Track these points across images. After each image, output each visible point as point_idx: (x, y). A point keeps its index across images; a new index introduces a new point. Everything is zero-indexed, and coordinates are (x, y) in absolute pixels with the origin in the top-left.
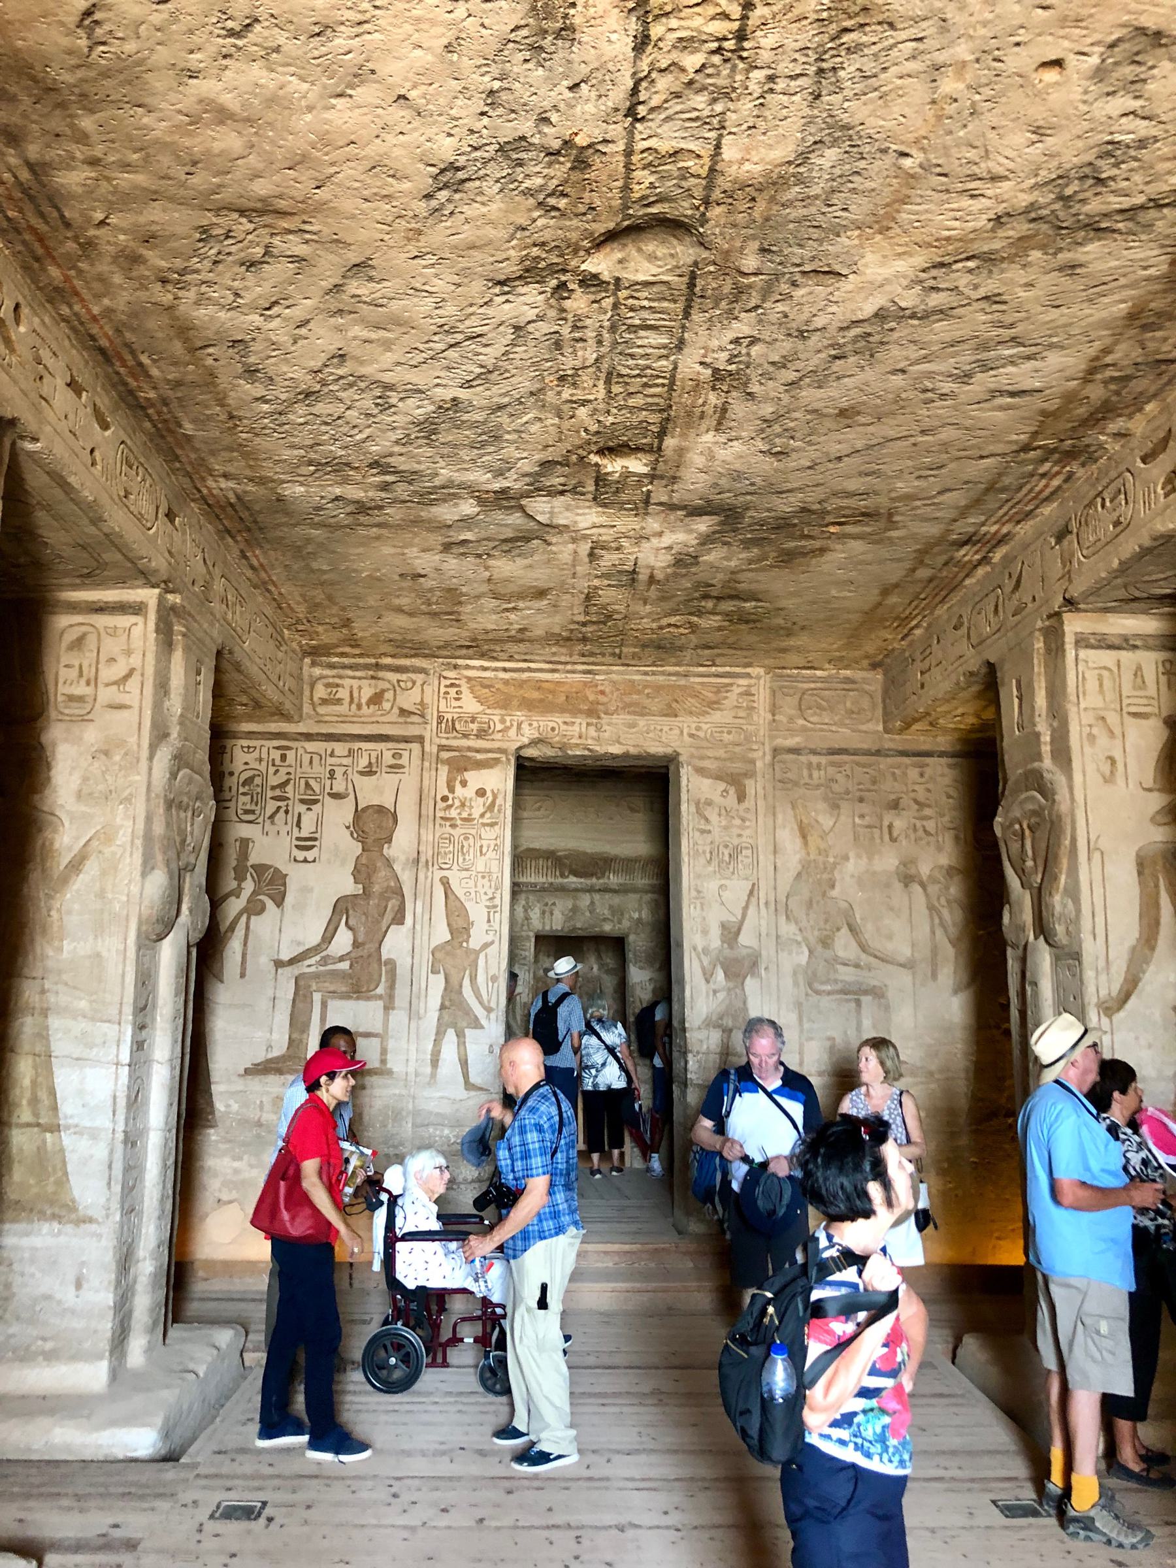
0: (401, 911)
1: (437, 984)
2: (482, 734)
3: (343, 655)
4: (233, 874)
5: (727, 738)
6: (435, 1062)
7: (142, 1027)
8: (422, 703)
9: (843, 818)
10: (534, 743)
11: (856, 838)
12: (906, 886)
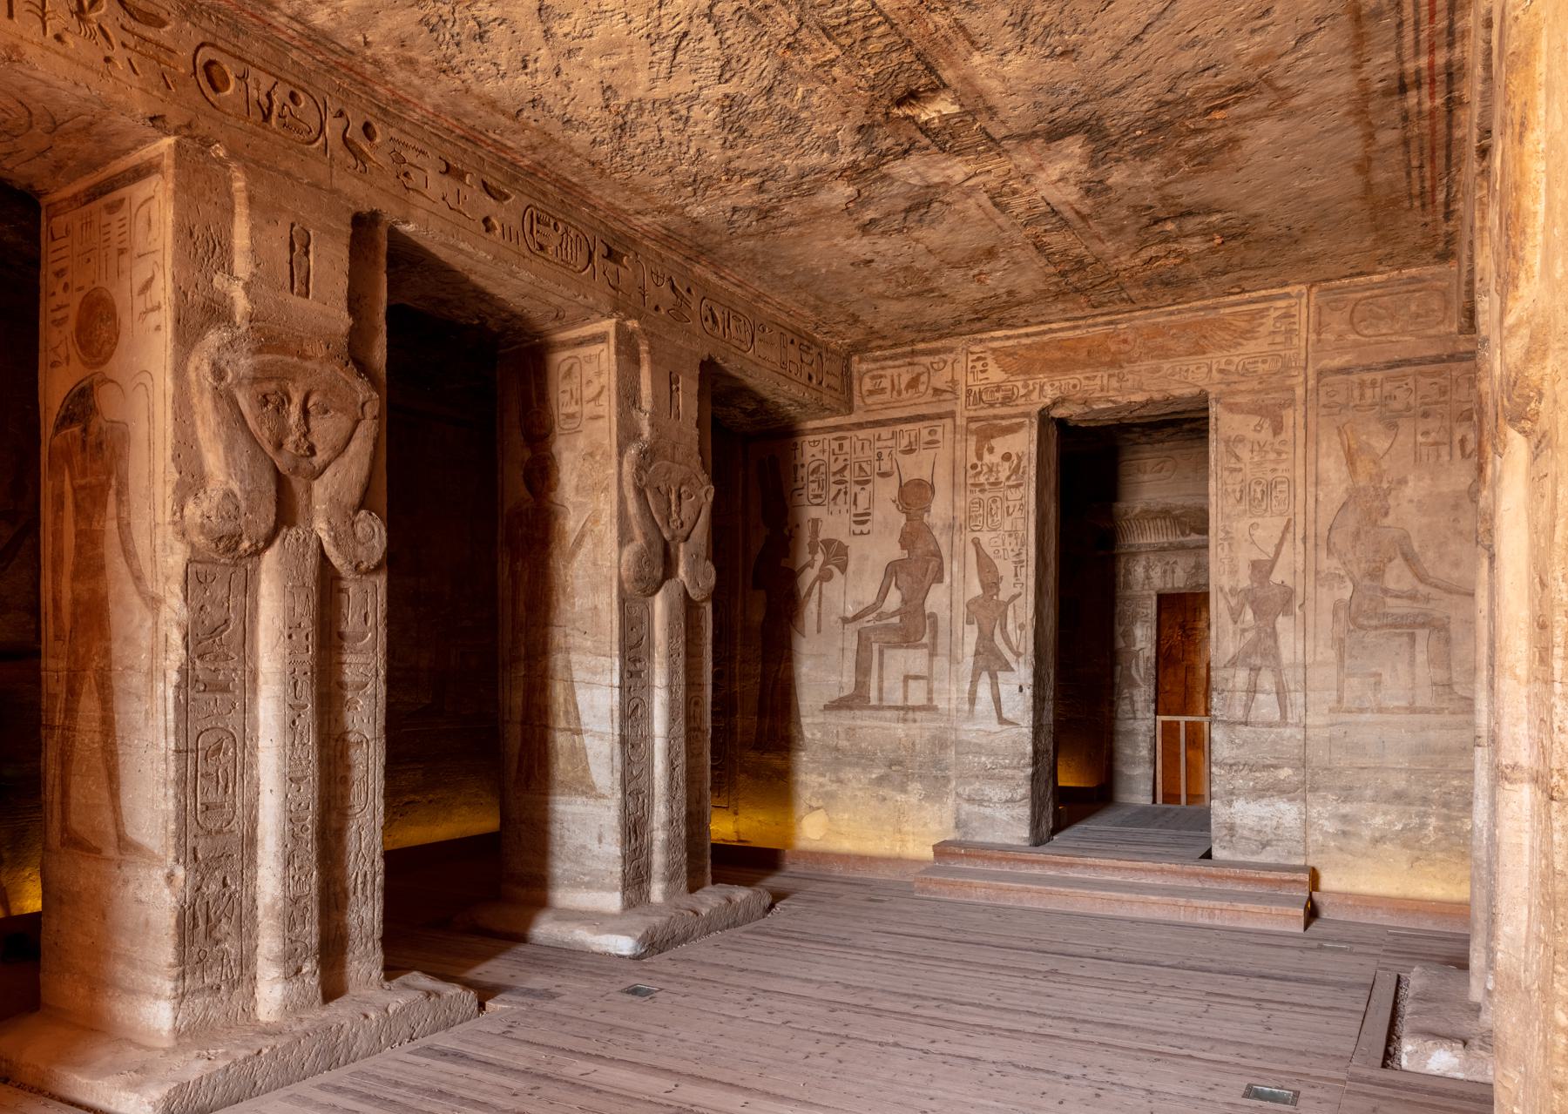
0: (941, 569)
1: (971, 636)
2: (1007, 401)
3: (880, 348)
5: (1261, 367)
6: (972, 700)
7: (635, 660)
8: (953, 381)
9: (1401, 438)
10: (1055, 404)
11: (1417, 458)
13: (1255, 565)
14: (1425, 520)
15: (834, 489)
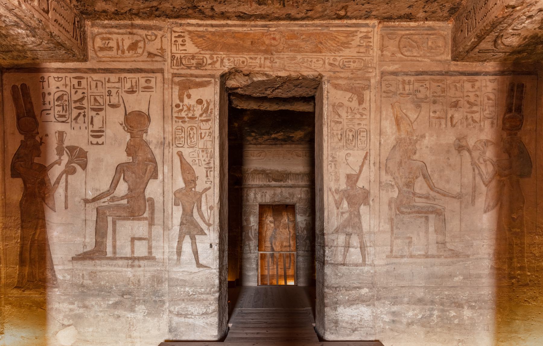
4: (55, 152)
9: (422, 113)
11: (430, 124)
12: (459, 152)
13: (348, 177)
14: (433, 158)
15: (75, 112)
